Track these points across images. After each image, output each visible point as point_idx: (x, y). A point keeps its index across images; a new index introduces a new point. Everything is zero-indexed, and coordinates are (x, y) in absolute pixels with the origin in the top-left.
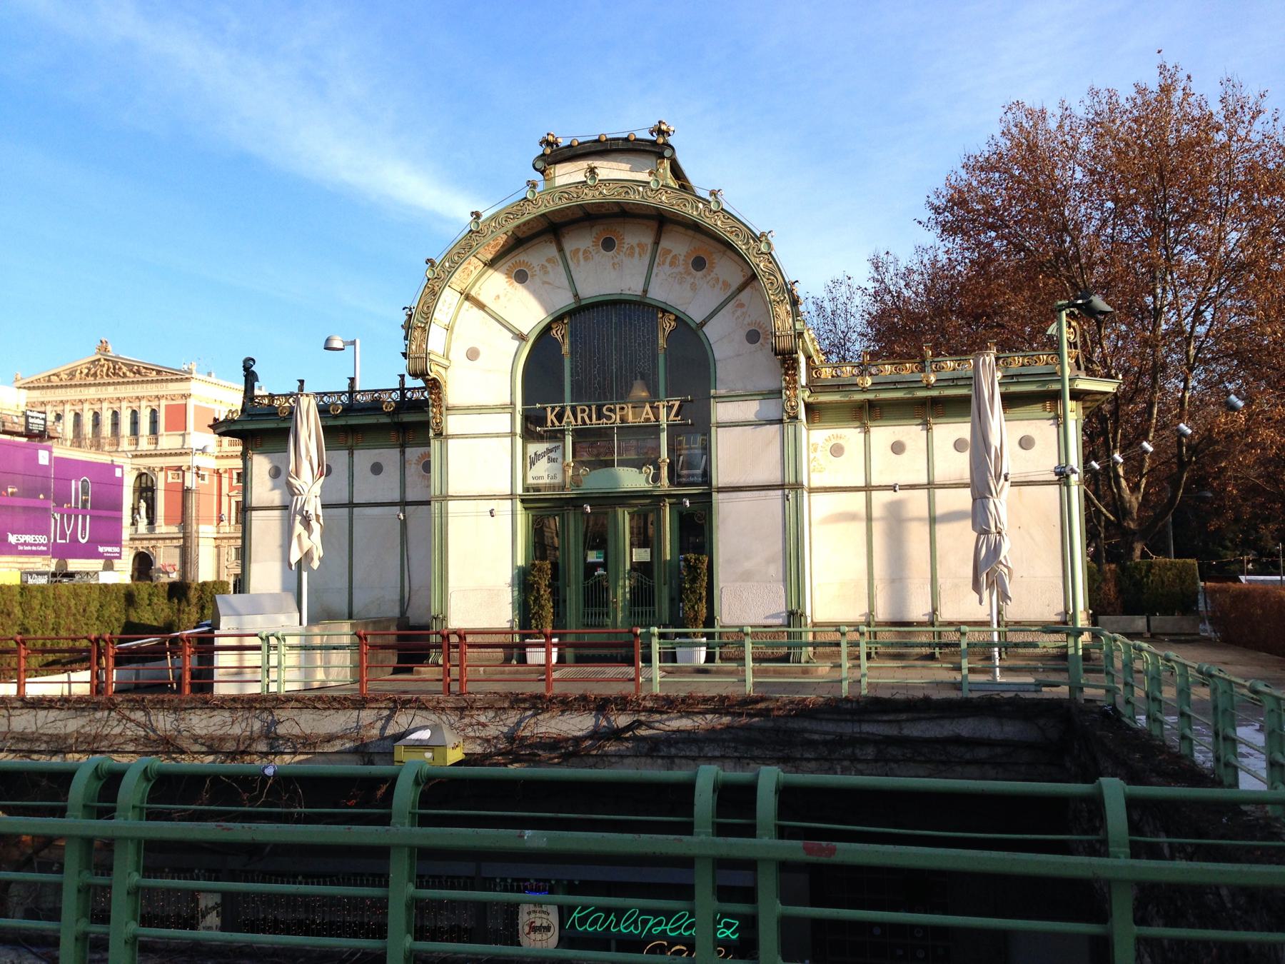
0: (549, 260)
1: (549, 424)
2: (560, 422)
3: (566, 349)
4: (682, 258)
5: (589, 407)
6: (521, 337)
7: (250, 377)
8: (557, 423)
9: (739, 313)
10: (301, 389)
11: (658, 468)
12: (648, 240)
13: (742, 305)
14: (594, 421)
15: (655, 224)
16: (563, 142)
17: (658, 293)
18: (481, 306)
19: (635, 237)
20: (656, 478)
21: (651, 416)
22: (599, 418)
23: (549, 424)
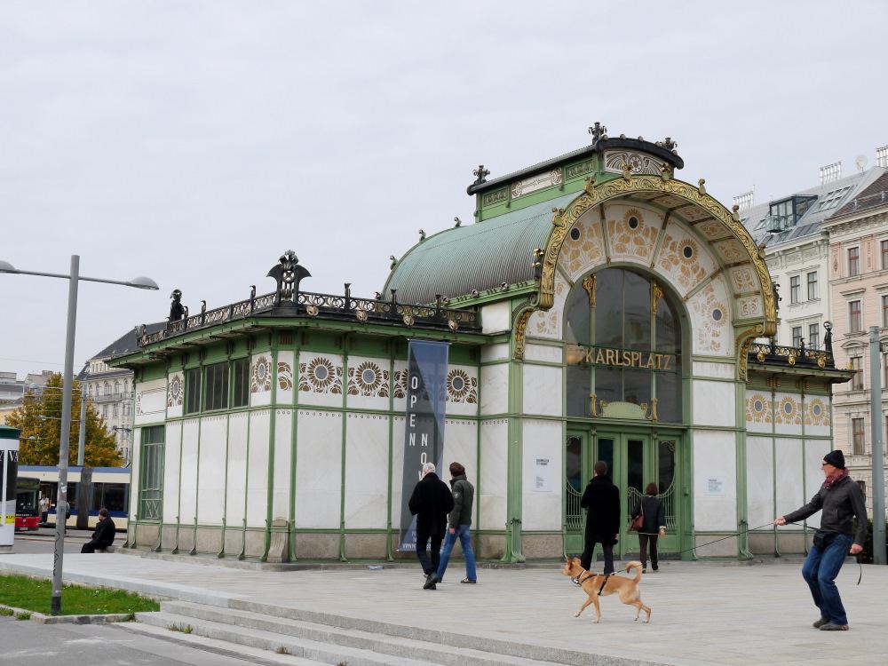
0: (594, 225)
4: (678, 245)
6: (572, 285)
7: (289, 269)
9: (709, 295)
10: (347, 292)
11: (650, 403)
12: (658, 226)
13: (712, 290)
15: (663, 214)
16: (612, 133)
17: (660, 270)
19: (651, 220)
20: (649, 412)
21: (653, 364)
22: (620, 361)
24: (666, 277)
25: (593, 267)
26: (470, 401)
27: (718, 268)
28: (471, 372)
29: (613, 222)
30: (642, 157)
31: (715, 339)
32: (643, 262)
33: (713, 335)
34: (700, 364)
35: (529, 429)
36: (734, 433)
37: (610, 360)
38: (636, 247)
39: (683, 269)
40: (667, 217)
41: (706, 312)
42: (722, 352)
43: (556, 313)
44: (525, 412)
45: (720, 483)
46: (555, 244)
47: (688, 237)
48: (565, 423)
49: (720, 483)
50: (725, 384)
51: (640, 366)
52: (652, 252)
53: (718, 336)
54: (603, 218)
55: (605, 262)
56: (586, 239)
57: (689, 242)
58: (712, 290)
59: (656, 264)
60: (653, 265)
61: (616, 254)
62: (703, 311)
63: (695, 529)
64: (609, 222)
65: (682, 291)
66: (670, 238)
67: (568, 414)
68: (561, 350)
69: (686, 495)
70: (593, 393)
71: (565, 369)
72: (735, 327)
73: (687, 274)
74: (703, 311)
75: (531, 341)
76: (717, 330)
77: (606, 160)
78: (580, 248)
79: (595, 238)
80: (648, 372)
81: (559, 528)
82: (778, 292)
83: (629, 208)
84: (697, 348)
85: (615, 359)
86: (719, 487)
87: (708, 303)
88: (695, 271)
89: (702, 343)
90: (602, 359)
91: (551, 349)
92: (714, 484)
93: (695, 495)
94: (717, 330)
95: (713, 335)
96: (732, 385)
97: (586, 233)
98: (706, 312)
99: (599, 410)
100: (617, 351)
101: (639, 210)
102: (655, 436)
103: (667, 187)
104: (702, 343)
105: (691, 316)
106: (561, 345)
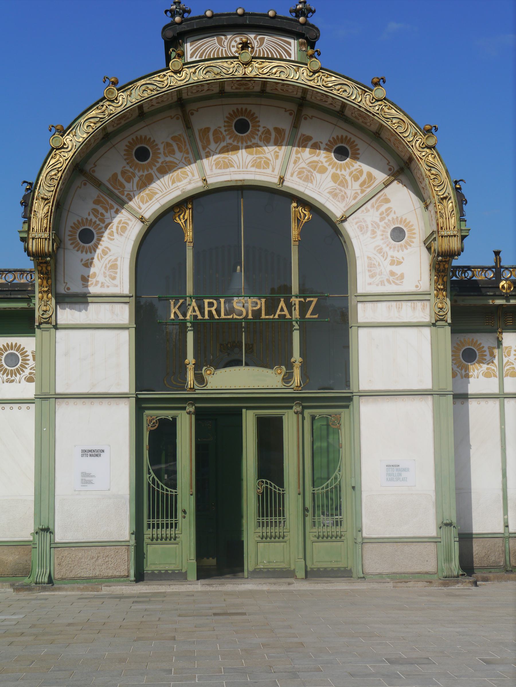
0: (174, 139)
1: (172, 316)
2: (185, 315)
3: (189, 235)
5: (217, 299)
6: (142, 219)
8: (181, 317)
11: (290, 366)
12: (286, 125)
13: (387, 201)
14: (223, 316)
15: (293, 107)
17: (294, 184)
18: (98, 184)
20: (288, 378)
21: (286, 312)
23: (172, 316)
24: (308, 192)
25: (177, 193)
26: (30, 380)
27: (396, 168)
28: (28, 343)
29: (208, 130)
30: (252, 36)
31: (394, 268)
32: (268, 177)
33: (392, 263)
34: (369, 305)
35: (65, 414)
36: (430, 397)
37: (210, 312)
38: (250, 157)
39: (335, 178)
40: (299, 111)
41: (379, 233)
42: (408, 286)
43: (116, 260)
44: (59, 390)
45: (406, 470)
46: (53, 173)
47: (339, 133)
48: (134, 400)
49: (406, 470)
50: (415, 330)
51: (263, 316)
52: (279, 162)
53: (399, 263)
54: (188, 126)
55: (200, 184)
56: (162, 159)
57: (342, 139)
58: (387, 201)
59: (287, 177)
60: (282, 179)
61: (216, 171)
62: (374, 232)
63: (365, 535)
64: (200, 131)
65: (335, 209)
66: (309, 138)
67: (136, 391)
68: (126, 307)
69: (354, 488)
70: (190, 359)
71: (133, 331)
72: (429, 249)
73: (343, 183)
74: (374, 232)
75: (67, 300)
76: (399, 255)
77: (189, 48)
78: (153, 171)
79: (178, 155)
80: (285, 326)
81: (127, 538)
82: (463, 191)
83: (234, 108)
84: (364, 282)
85: (218, 311)
86: (404, 474)
87: (382, 219)
88: (356, 178)
89: (372, 276)
90: (198, 313)
91: (107, 306)
92: (395, 471)
93: (363, 488)
94: (399, 255)
95: (392, 263)
96: (427, 332)
97: (162, 150)
98: (379, 233)
99: (200, 379)
100: (222, 301)
101: (249, 108)
102: (299, 409)
103: (248, 70)
104: (372, 276)
105: (354, 241)
106: (127, 300)
